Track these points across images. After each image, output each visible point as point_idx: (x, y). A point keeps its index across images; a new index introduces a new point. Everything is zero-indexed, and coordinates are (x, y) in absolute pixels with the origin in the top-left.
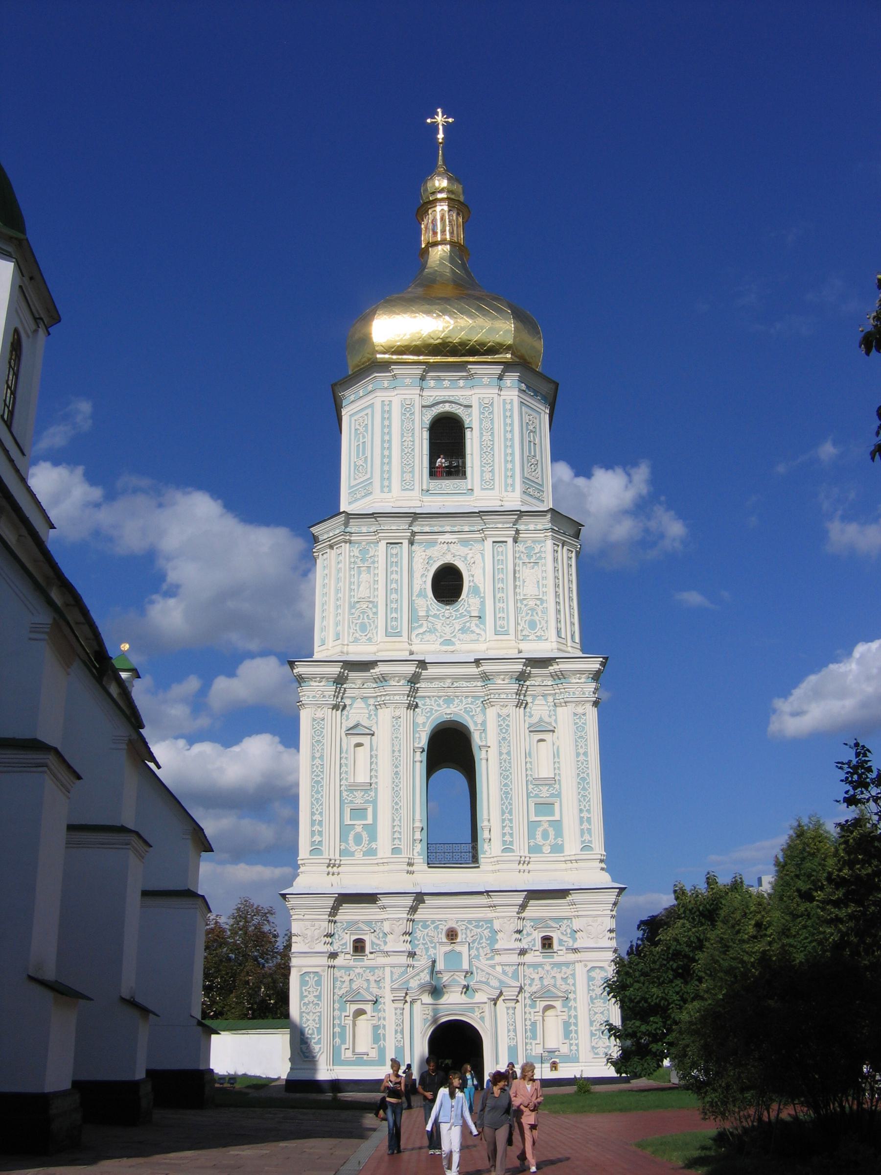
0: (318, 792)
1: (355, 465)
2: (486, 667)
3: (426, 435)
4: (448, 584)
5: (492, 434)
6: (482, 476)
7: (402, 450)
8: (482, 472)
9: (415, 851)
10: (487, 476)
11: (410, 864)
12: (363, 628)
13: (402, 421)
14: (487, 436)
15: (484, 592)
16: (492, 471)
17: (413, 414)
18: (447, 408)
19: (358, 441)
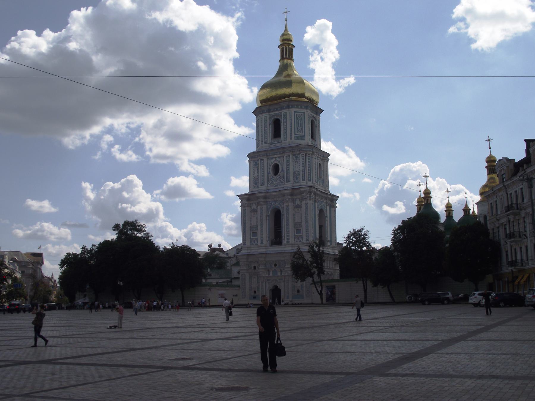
2: (283, 192)
4: (276, 169)
10: (285, 136)
14: (285, 124)
18: (276, 117)
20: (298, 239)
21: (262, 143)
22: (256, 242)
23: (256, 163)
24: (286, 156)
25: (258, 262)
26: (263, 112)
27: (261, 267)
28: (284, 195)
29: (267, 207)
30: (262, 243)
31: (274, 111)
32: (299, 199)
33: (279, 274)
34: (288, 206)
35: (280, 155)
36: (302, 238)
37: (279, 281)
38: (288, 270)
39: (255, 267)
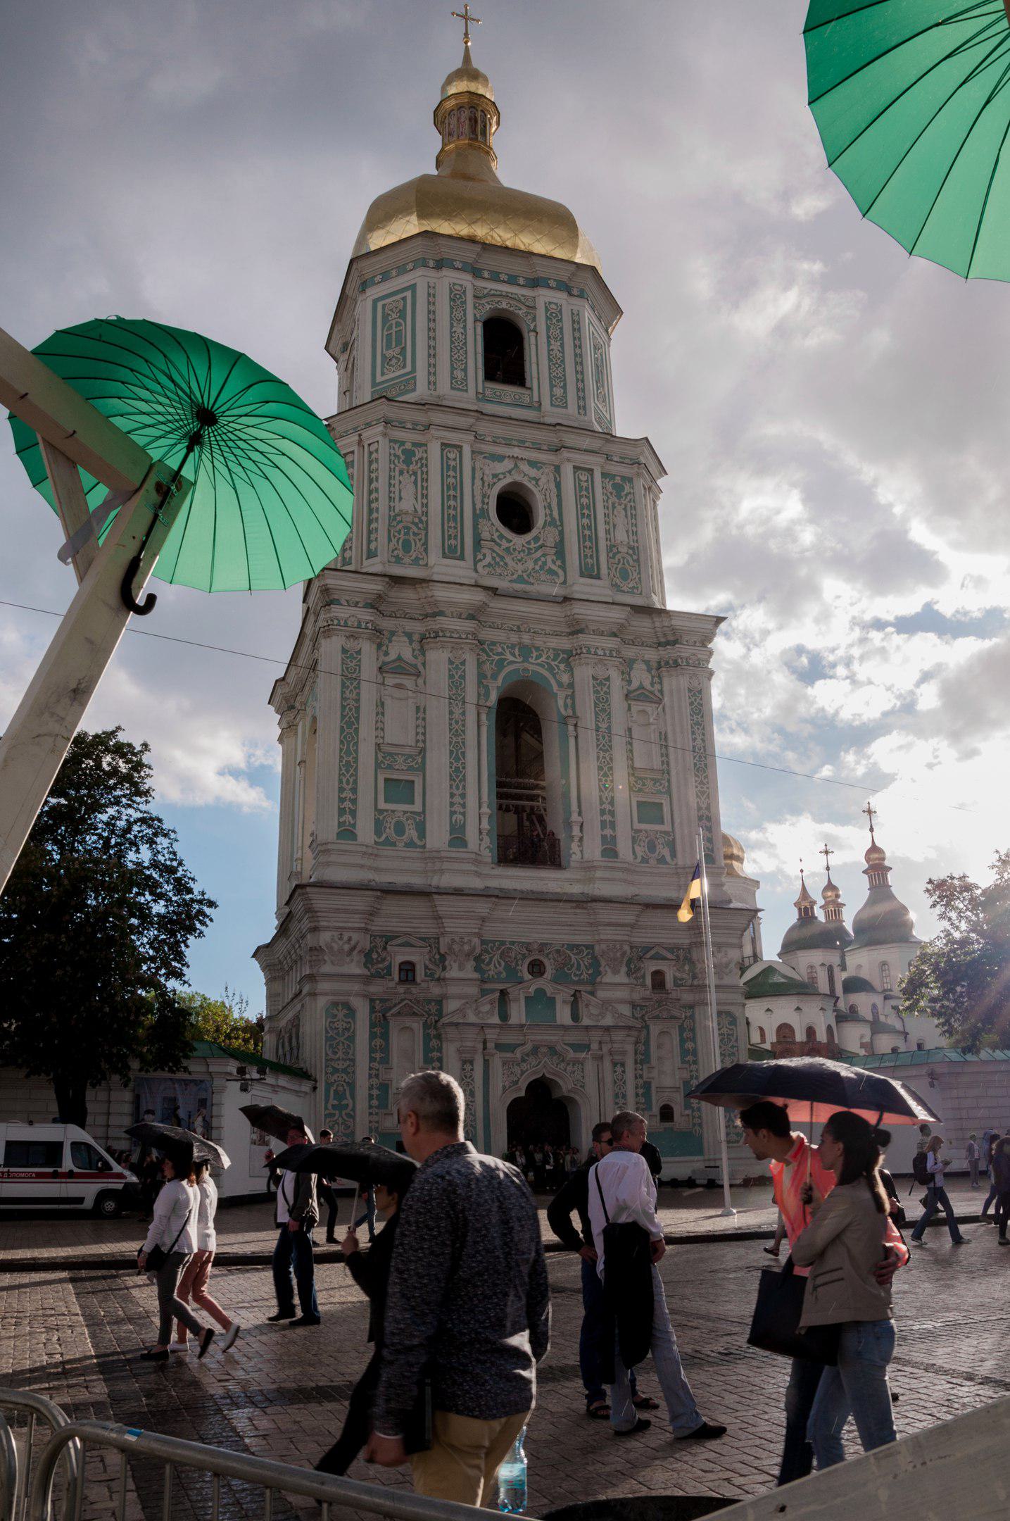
0: (348, 753)
1: (383, 356)
3: (480, 330)
5: (562, 345)
6: (551, 390)
7: (452, 342)
8: (552, 386)
9: (484, 845)
11: (477, 862)
12: (407, 546)
13: (452, 308)
14: (556, 346)
15: (562, 525)
16: (564, 387)
17: (465, 302)
18: (504, 305)
19: (390, 328)
20: (652, 847)
21: (432, 384)
22: (411, 833)
23: (409, 454)
24: (575, 467)
25: (432, 942)
26: (439, 265)
27: (454, 972)
28: (576, 629)
29: (480, 664)
30: (458, 838)
31: (495, 277)
32: (647, 662)
33: (563, 1015)
34: (601, 683)
35: (535, 455)
36: (672, 846)
37: (571, 1054)
38: (617, 990)
39: (408, 970)
